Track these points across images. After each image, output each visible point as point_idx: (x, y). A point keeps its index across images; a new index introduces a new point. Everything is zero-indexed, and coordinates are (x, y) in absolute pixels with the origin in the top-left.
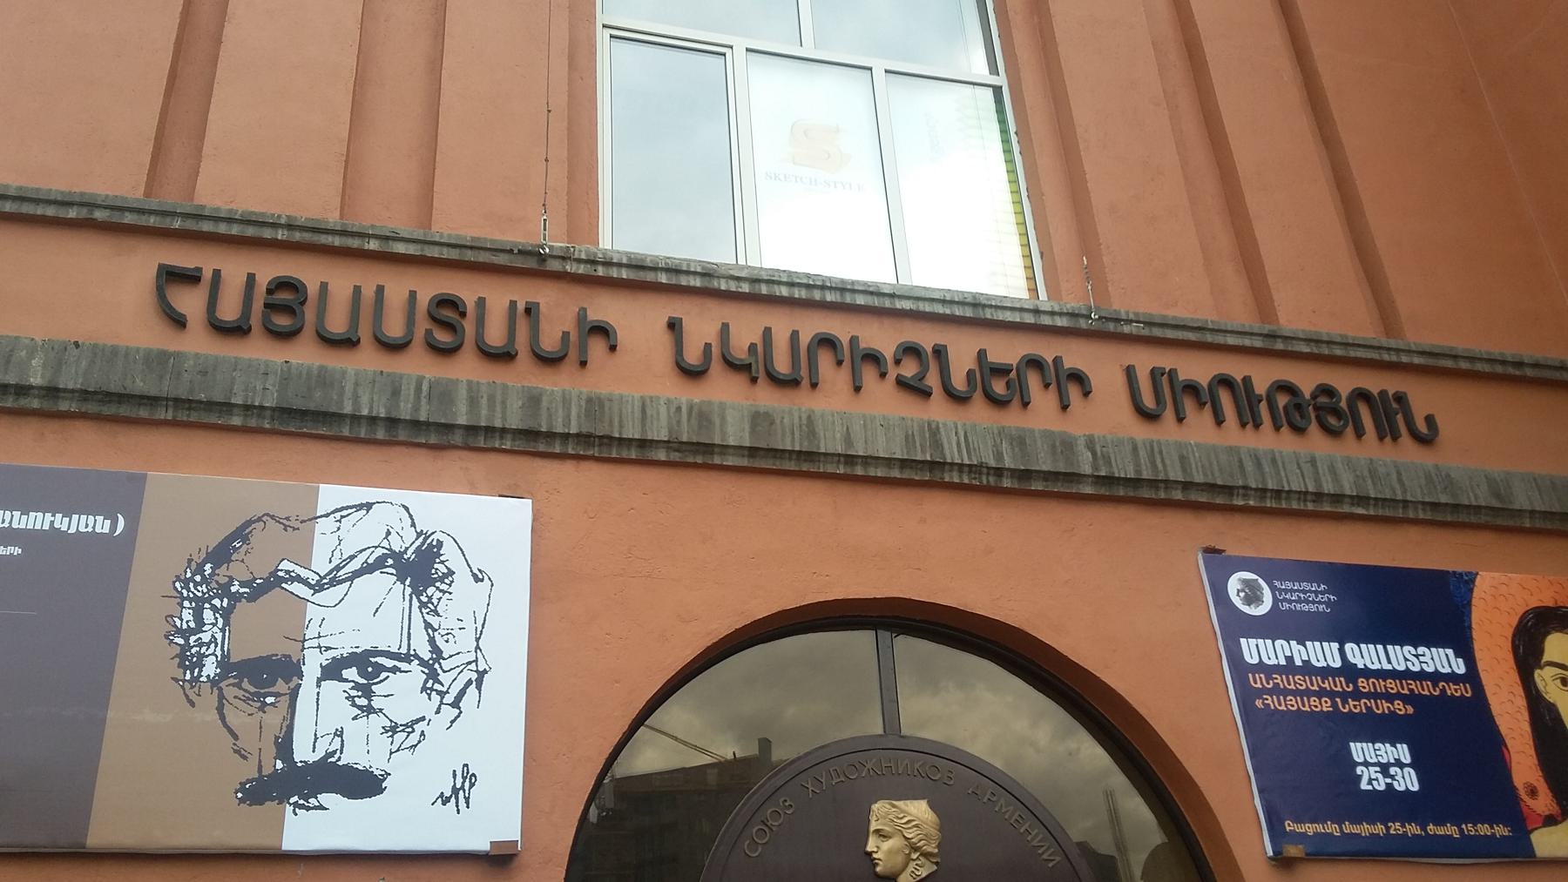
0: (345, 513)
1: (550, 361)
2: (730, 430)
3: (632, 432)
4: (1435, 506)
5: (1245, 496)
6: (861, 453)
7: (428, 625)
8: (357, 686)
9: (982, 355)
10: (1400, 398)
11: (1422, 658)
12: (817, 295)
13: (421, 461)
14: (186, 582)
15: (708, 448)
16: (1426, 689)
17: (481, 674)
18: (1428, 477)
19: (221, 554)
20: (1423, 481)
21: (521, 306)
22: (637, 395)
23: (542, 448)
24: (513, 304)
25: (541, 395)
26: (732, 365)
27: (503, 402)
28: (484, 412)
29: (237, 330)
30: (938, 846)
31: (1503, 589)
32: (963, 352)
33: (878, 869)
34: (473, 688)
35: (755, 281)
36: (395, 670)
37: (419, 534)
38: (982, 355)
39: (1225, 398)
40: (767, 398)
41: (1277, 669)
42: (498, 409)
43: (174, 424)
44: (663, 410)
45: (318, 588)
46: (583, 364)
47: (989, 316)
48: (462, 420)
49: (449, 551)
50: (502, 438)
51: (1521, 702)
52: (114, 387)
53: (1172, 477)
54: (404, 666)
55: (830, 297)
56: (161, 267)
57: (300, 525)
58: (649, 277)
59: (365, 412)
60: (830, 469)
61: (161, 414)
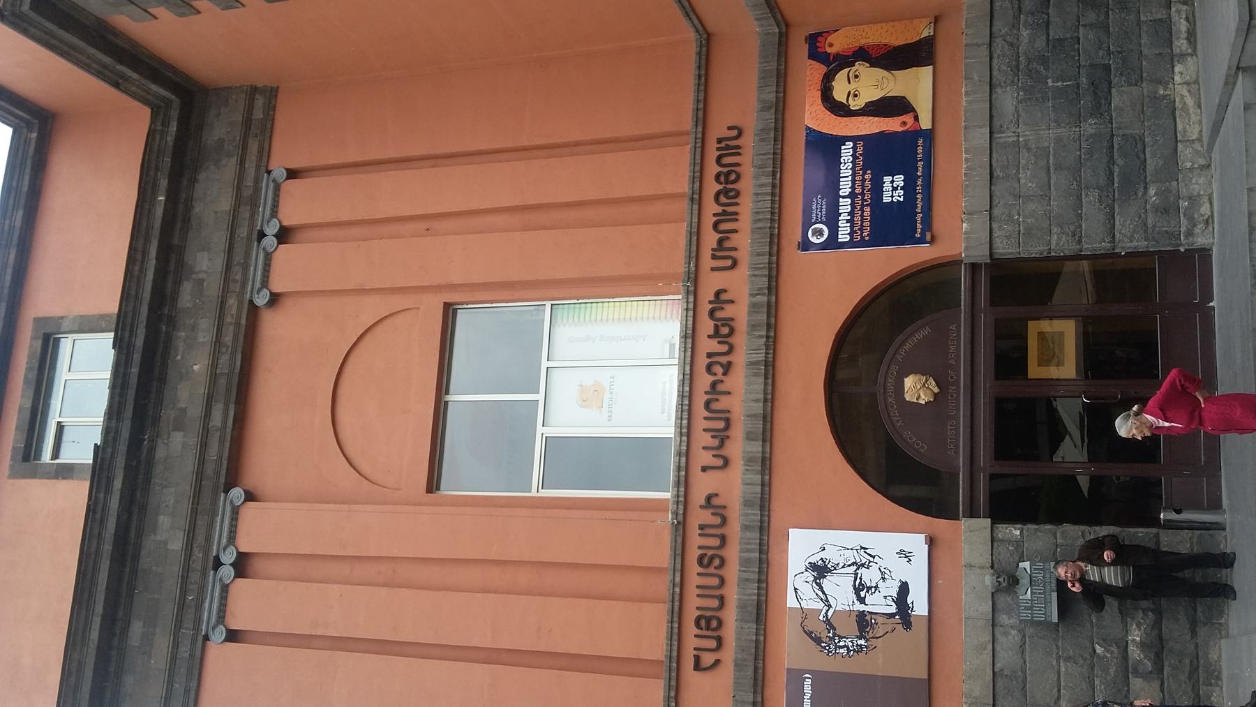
0: (799, 598)
1: (724, 521)
2: (754, 450)
3: (759, 489)
4: (775, 140)
5: (774, 228)
6: (763, 396)
7: (843, 567)
8: (868, 592)
9: (709, 337)
10: (719, 141)
11: (846, 161)
12: (686, 408)
13: (773, 570)
14: (829, 652)
15: (764, 459)
16: (860, 162)
17: (862, 548)
18: (762, 140)
19: (818, 641)
20: (764, 143)
21: (700, 532)
22: (742, 486)
23: (766, 524)
24: (700, 535)
25: (744, 525)
26: (722, 445)
27: (748, 539)
28: (753, 546)
29: (719, 640)
30: (923, 375)
31: (813, 114)
32: (708, 345)
33: (932, 400)
34: (866, 551)
35: (681, 434)
36: (861, 579)
37: (806, 571)
38: (709, 337)
39: (723, 227)
40: (738, 432)
41: (852, 227)
42: (750, 541)
43: (764, 660)
44: (748, 476)
45: (830, 606)
46: (725, 507)
47: (691, 332)
48: (757, 555)
49: (813, 560)
50: (763, 540)
51: (865, 119)
52: (752, 682)
53: (767, 261)
54: (859, 576)
55: (686, 402)
56: (694, 670)
57: (805, 614)
58: (682, 479)
59: (756, 591)
60: (769, 409)
61: (761, 665)
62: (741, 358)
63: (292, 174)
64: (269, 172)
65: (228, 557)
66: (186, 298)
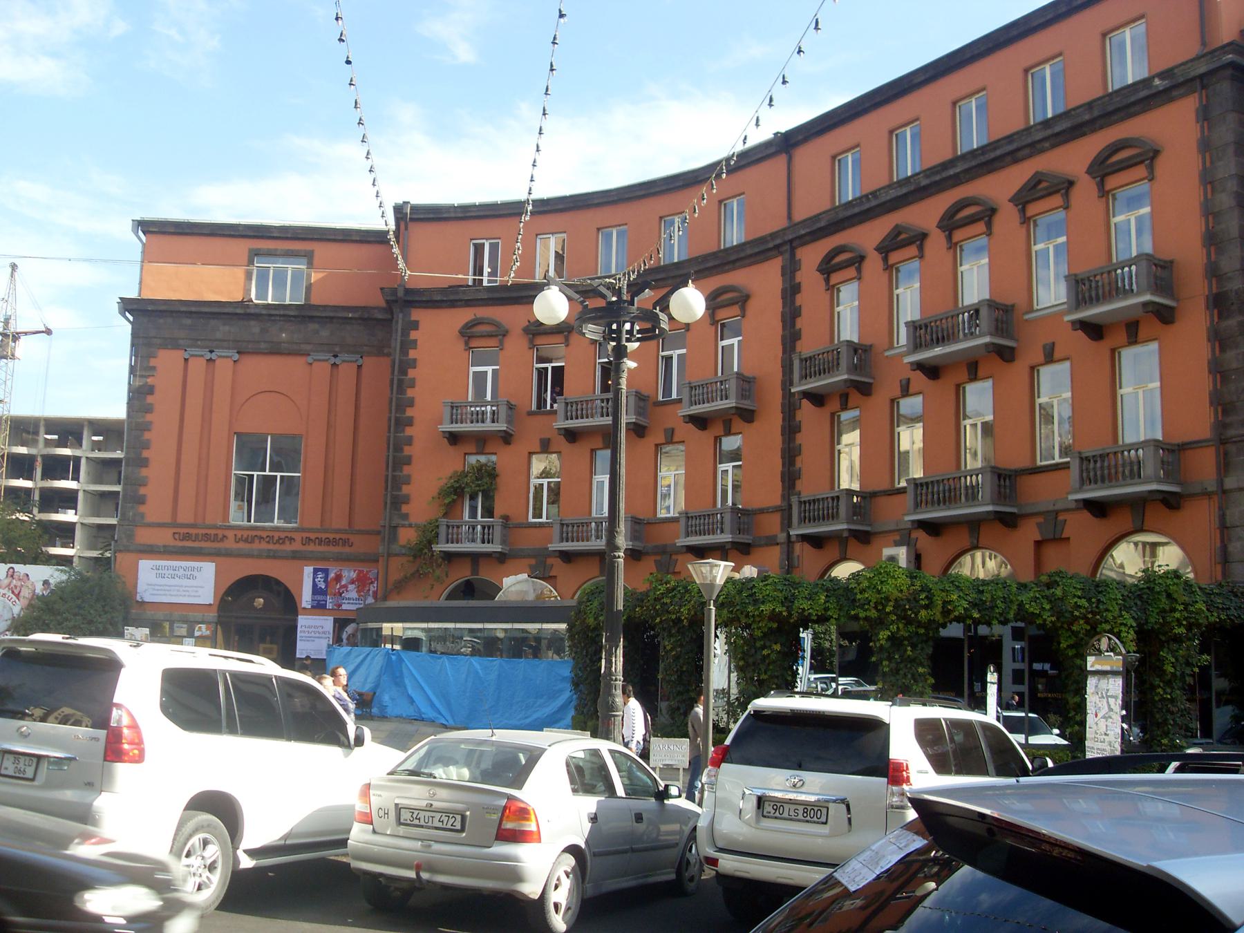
1: (218, 542)
32: (276, 535)
62: (271, 547)
63: (359, 367)
64: (361, 357)
65: (214, 356)
66: (313, 326)
